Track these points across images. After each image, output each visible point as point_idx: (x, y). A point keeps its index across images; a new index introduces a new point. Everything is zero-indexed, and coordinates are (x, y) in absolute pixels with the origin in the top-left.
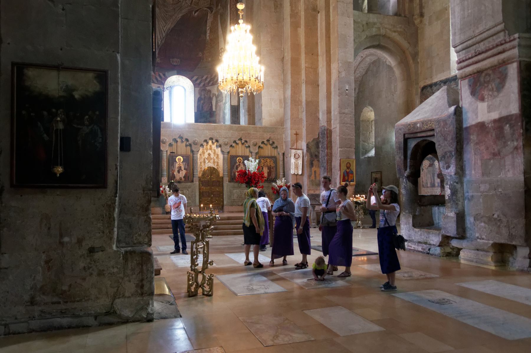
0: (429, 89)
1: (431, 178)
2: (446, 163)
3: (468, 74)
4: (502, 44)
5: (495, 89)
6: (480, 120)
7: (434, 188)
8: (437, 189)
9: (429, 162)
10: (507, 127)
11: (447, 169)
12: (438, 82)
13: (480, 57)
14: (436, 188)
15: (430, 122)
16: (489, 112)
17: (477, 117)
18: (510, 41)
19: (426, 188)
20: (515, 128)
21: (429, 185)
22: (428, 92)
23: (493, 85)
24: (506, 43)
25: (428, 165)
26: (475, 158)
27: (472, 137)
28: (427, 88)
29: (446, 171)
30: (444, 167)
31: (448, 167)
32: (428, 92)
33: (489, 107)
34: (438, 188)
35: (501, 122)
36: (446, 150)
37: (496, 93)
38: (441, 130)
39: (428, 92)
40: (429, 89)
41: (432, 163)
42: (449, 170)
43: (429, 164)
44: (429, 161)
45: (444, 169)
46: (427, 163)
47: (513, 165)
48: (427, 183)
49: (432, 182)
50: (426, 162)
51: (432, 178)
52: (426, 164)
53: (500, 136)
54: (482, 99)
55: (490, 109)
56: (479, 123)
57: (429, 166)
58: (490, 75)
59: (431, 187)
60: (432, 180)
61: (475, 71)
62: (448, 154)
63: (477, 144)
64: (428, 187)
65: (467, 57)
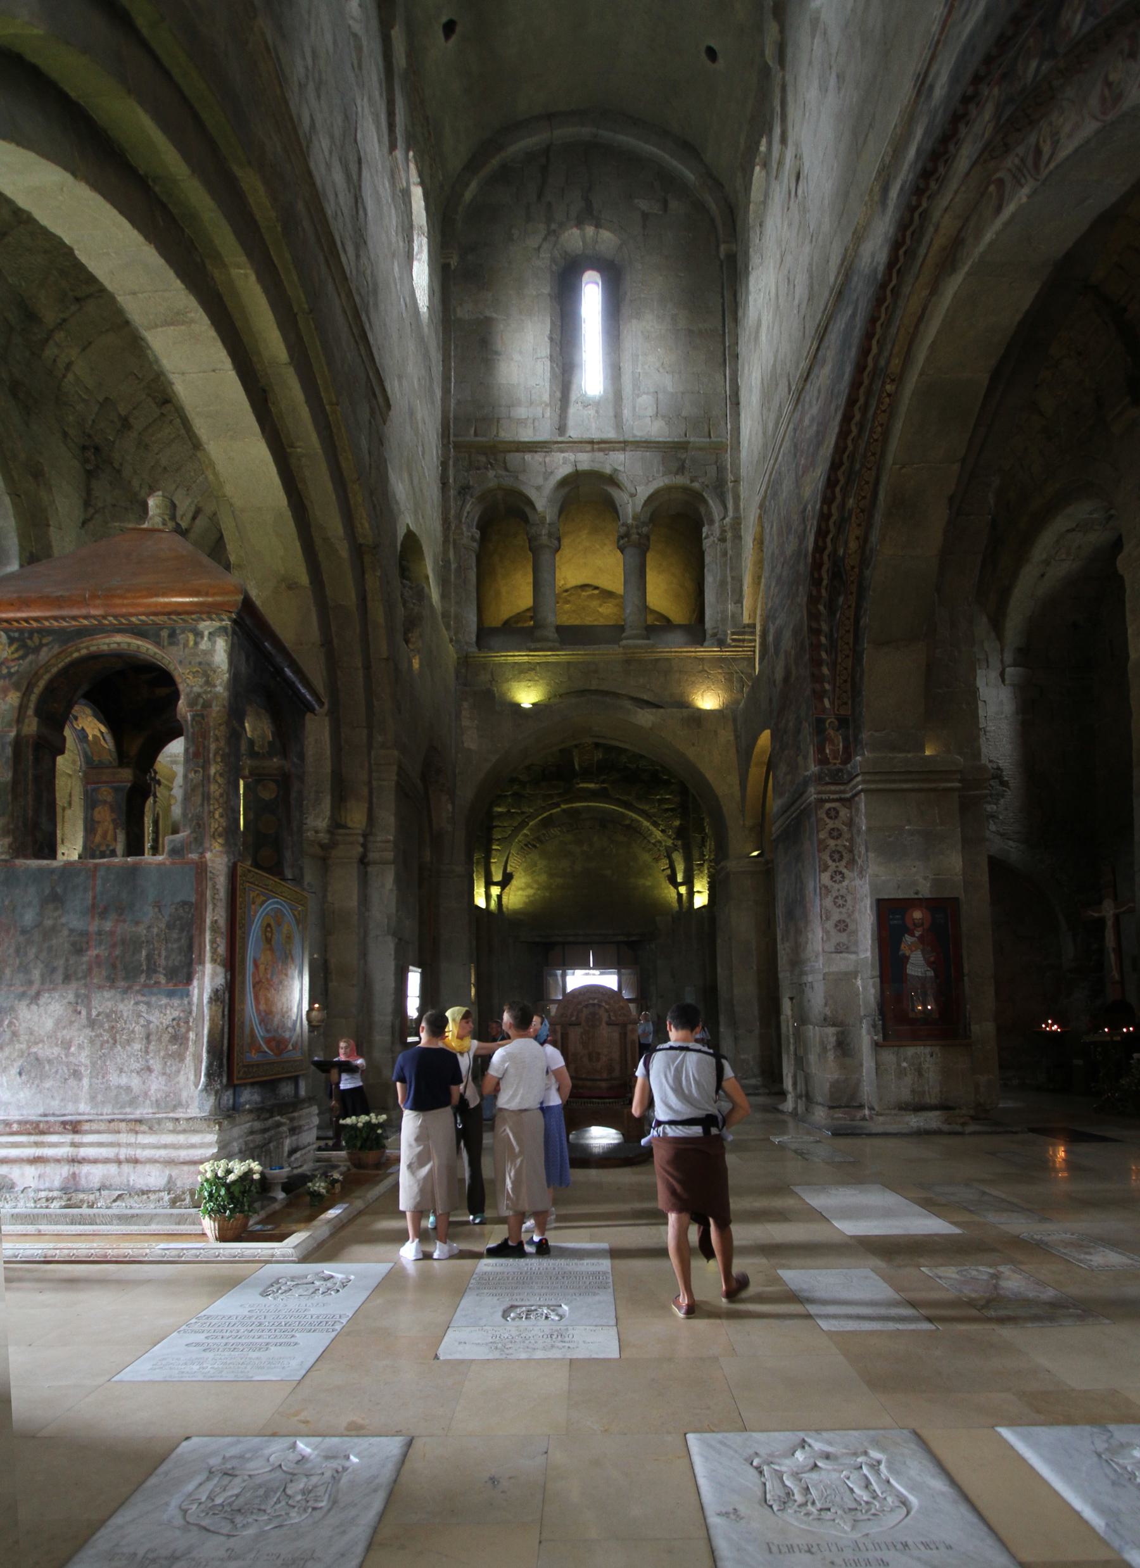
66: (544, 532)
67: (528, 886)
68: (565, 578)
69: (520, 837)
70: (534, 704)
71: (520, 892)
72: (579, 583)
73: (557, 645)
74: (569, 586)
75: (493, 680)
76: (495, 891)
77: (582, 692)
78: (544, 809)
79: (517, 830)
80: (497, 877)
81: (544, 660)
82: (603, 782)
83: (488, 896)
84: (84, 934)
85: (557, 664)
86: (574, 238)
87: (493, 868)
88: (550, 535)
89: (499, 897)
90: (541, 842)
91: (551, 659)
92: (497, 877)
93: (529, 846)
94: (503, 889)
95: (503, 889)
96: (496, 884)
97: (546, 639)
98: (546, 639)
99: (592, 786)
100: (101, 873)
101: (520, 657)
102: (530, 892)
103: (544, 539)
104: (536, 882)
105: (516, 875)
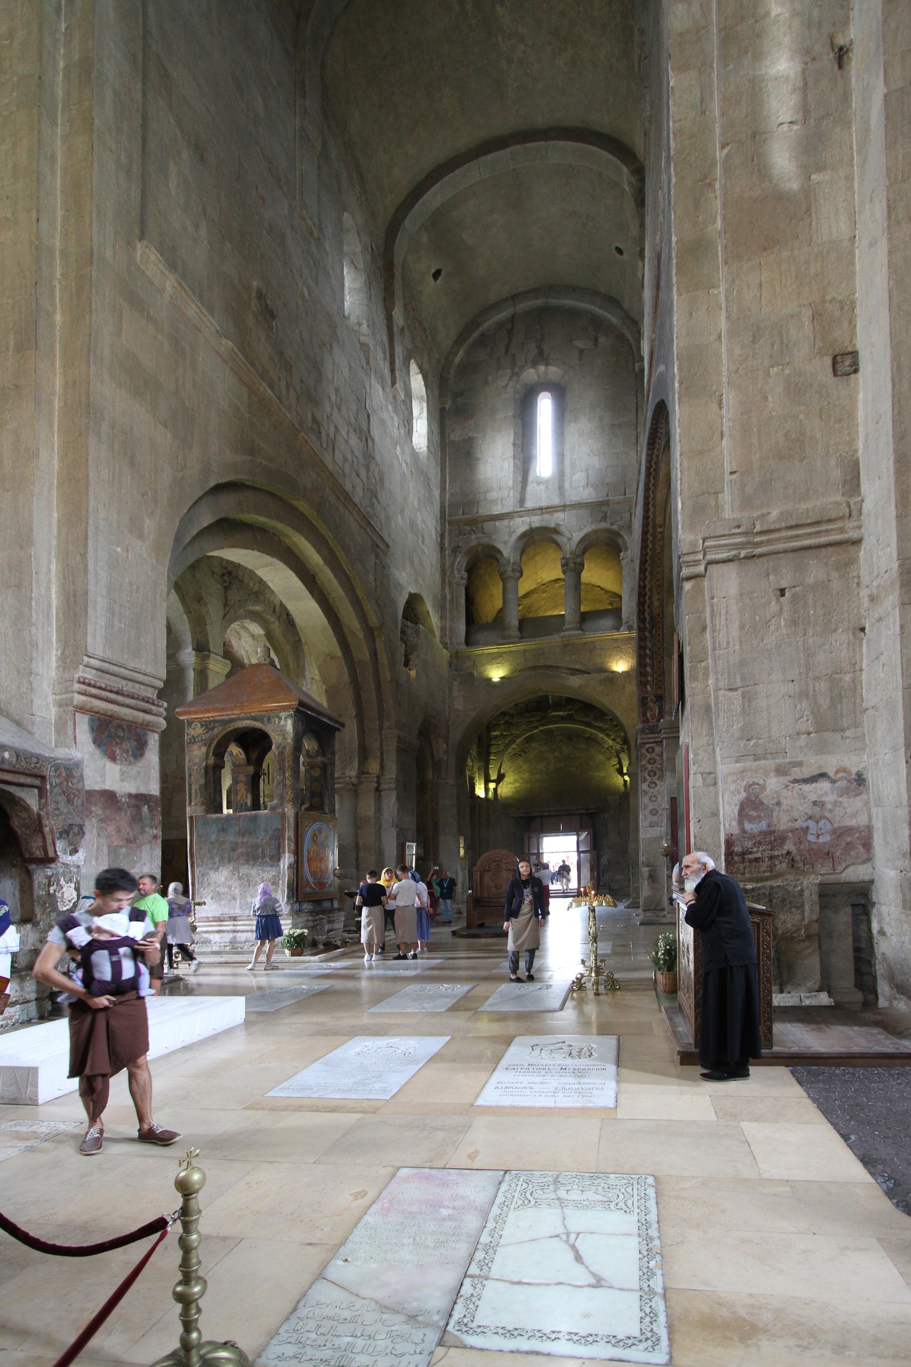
2: (70, 844)
3: (95, 709)
4: (148, 702)
5: (130, 753)
6: (108, 786)
10: (145, 809)
11: (71, 854)
13: (120, 698)
15: (35, 760)
16: (122, 780)
17: (104, 781)
18: (158, 706)
20: (154, 812)
23: (126, 745)
24: (153, 704)
26: (98, 842)
27: (93, 809)
29: (70, 858)
30: (65, 850)
31: (75, 851)
33: (122, 773)
35: (140, 799)
36: (70, 821)
37: (131, 759)
38: (61, 783)
42: (76, 857)
45: (65, 854)
47: (152, 860)
53: (137, 818)
54: (113, 758)
55: (123, 777)
56: (106, 791)
58: (123, 730)
61: (109, 713)
62: (76, 829)
63: (102, 820)
65: (98, 684)
66: (510, 569)
67: (516, 781)
68: (541, 578)
69: (510, 750)
70: (501, 678)
71: (509, 786)
72: (553, 578)
73: (517, 640)
74: (545, 581)
75: (474, 665)
76: (492, 786)
77: (534, 668)
78: (527, 731)
79: (507, 746)
80: (494, 777)
81: (508, 650)
82: (570, 710)
83: (487, 790)
84: (236, 843)
85: (517, 652)
86: (530, 375)
87: (491, 772)
88: (513, 571)
89: (495, 790)
90: (525, 752)
91: (513, 649)
92: (494, 777)
93: (516, 756)
94: (497, 784)
95: (497, 784)
96: (493, 781)
97: (510, 637)
98: (510, 637)
99: (561, 713)
100: (242, 818)
101: (493, 649)
102: (517, 785)
103: (510, 573)
104: (521, 778)
105: (507, 775)
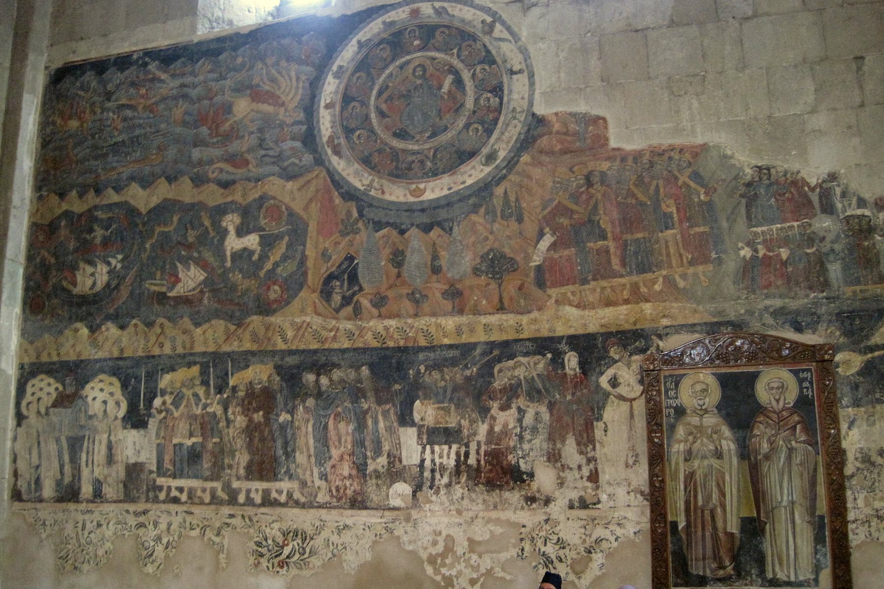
0: (89, 77)
1: (60, 458)
7: (72, 506)
8: (90, 512)
9: (55, 384)
12: (135, 57)
14: (83, 506)
19: (29, 505)
21: (48, 491)
22: (84, 88)
25: (48, 401)
28: (83, 74)
32: (84, 88)
34: (91, 506)
39: (82, 88)
40: (89, 77)
41: (70, 390)
43: (54, 395)
44: (57, 380)
46: (47, 389)
48: (38, 481)
49: (67, 479)
50: (42, 385)
51: (66, 458)
52: (39, 394)
57: (55, 405)
59: (60, 500)
60: (67, 468)
64: (41, 500)
